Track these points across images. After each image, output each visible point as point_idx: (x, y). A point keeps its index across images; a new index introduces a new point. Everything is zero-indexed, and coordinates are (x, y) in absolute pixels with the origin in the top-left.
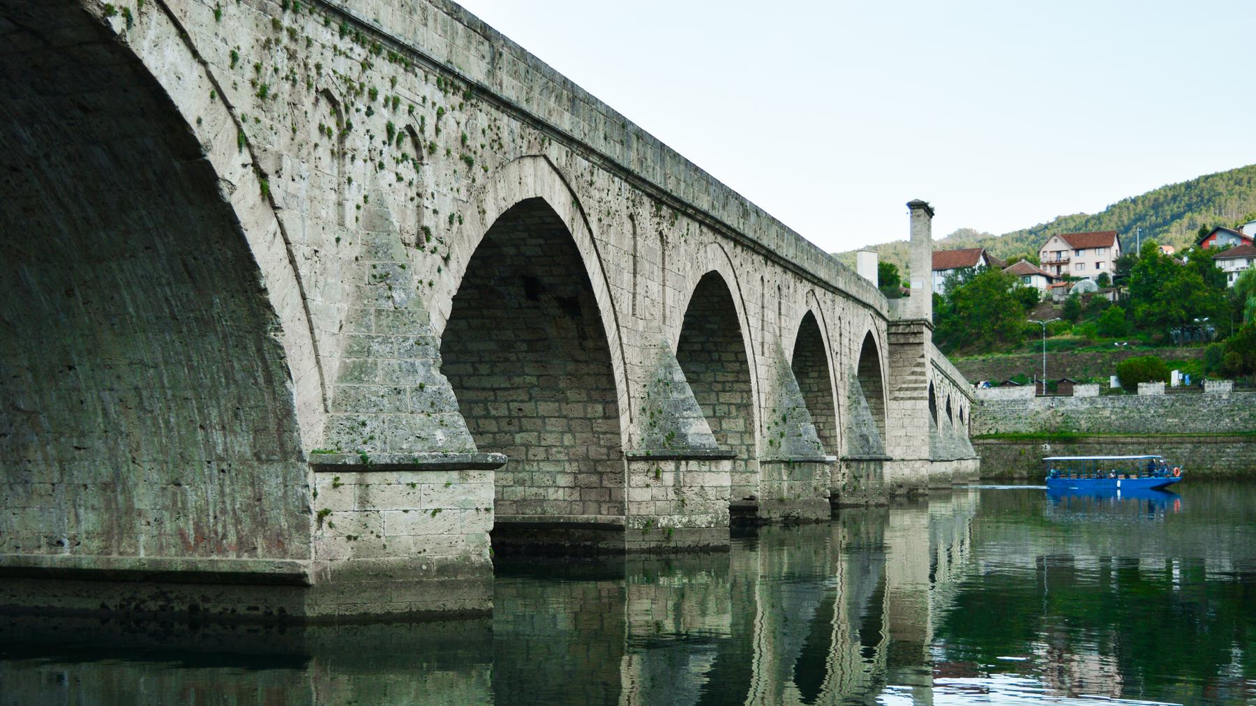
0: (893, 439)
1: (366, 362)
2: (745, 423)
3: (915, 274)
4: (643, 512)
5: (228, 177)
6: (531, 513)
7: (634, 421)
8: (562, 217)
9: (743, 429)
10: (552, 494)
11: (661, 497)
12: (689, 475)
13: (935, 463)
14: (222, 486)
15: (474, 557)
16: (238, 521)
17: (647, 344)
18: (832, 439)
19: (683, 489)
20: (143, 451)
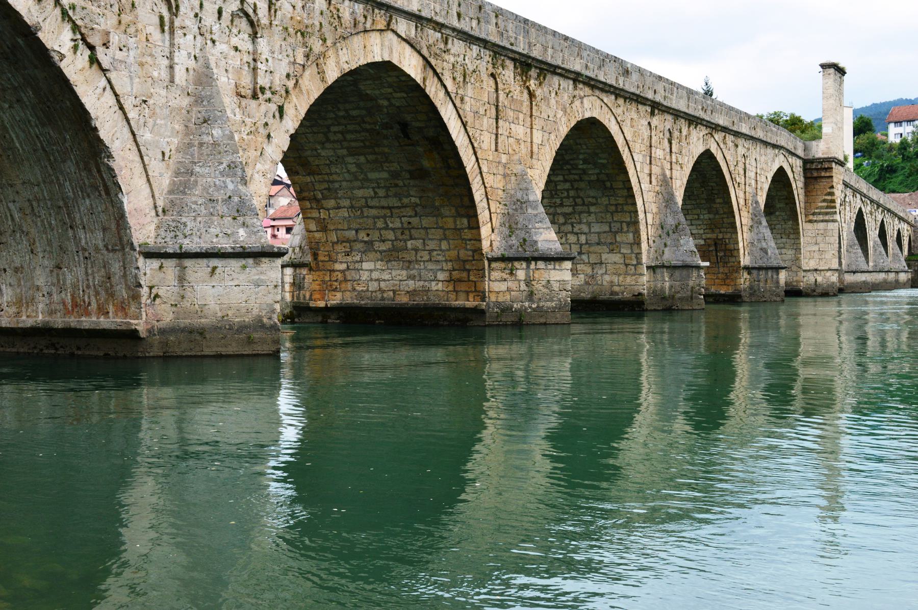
0: (808, 253)
1: (190, 180)
2: (634, 237)
3: (826, 121)
4: (501, 299)
5: (56, 48)
6: (419, 300)
7: (496, 231)
8: (413, 76)
9: (632, 241)
10: (434, 286)
11: (515, 288)
12: (537, 272)
13: (856, 274)
14: (86, 268)
15: (265, 320)
16: (97, 293)
17: (509, 172)
18: (736, 251)
19: (533, 283)
20: (37, 244)
